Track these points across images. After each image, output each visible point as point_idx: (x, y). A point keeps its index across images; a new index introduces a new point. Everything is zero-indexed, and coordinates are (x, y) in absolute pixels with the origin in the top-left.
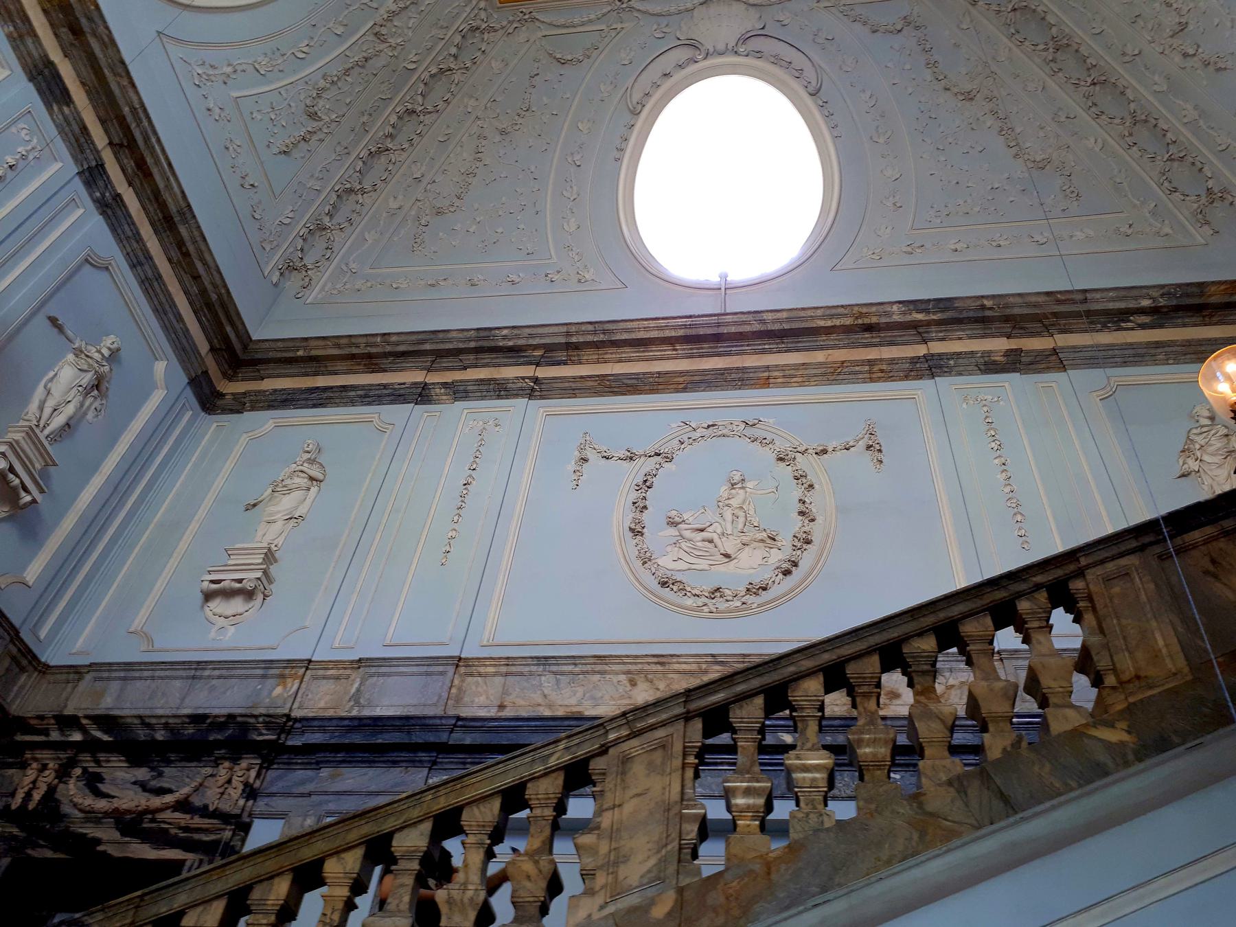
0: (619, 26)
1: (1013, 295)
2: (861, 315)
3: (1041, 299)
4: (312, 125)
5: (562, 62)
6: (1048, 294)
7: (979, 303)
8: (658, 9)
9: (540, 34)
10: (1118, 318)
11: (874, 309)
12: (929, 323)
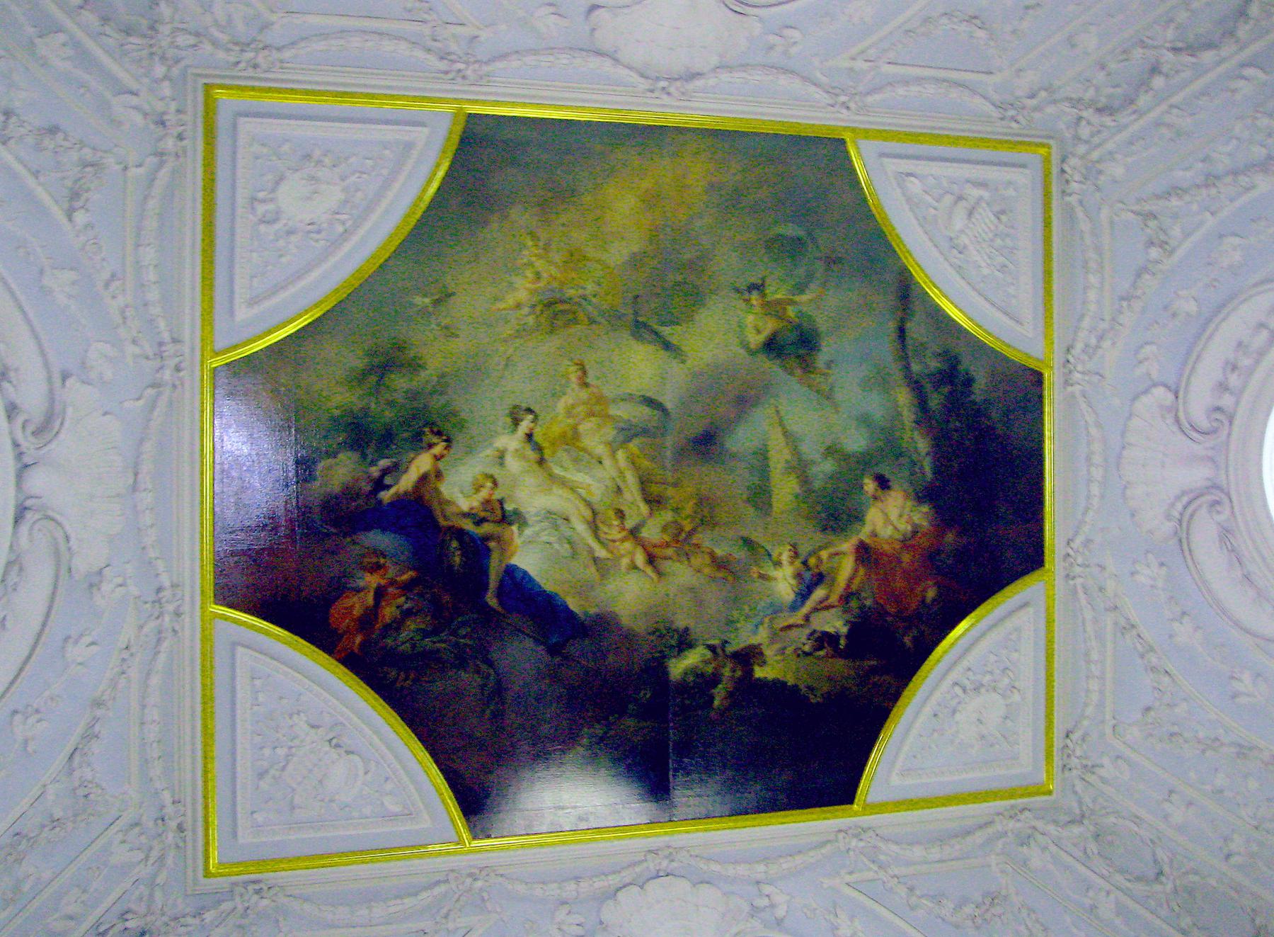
0: (860, 65)
8: (783, 81)
9: (997, 78)
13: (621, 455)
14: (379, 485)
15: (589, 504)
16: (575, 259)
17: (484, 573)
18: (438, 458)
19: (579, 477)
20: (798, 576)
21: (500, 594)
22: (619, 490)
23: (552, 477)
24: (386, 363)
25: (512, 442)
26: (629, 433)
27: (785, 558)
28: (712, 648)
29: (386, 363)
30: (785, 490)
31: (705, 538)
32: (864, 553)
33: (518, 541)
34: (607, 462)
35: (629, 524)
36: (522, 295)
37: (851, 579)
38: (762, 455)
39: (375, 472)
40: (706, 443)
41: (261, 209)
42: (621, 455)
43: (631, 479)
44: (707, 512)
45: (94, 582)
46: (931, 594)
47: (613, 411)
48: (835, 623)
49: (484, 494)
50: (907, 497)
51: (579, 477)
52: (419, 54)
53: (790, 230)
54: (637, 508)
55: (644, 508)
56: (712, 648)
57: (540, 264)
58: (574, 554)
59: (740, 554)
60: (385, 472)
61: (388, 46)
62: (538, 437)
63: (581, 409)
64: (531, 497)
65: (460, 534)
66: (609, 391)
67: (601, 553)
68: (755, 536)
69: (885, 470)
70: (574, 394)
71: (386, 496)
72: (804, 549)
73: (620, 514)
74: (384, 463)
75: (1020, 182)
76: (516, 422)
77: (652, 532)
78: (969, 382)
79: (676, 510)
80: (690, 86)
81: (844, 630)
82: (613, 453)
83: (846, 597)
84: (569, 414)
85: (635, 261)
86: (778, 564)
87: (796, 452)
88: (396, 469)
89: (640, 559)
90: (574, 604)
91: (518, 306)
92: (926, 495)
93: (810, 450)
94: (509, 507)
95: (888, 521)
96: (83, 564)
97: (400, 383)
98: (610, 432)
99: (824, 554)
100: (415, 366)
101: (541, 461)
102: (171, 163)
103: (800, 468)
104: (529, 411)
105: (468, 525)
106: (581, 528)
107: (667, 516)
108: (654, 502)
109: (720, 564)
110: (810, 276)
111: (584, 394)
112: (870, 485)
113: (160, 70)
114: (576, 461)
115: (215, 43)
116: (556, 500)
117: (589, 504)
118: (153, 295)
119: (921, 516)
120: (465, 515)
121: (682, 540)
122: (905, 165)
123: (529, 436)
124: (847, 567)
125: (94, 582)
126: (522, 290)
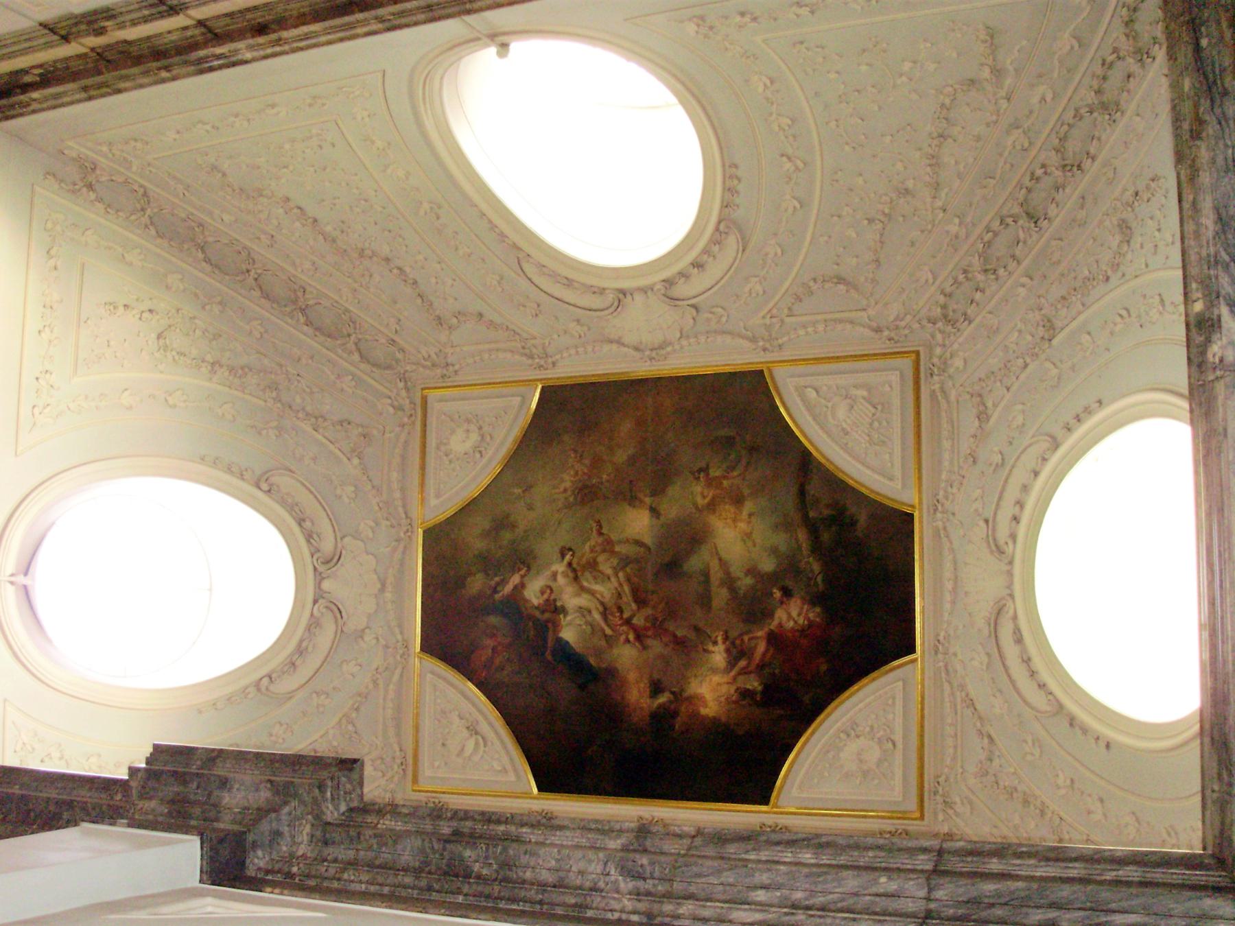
0: (768, 321)
1: (150, 85)
2: (278, 42)
3: (122, 85)
4: (1128, 215)
5: (840, 280)
6: (119, 91)
7: (175, 72)
9: (871, 312)
10: (50, 77)
11: (269, 51)
12: (205, 45)
13: (621, 574)
14: (495, 590)
15: (602, 604)
16: (597, 462)
17: (545, 640)
18: (522, 577)
19: (597, 587)
20: (728, 651)
21: (554, 653)
22: (619, 596)
23: (583, 589)
24: (502, 524)
25: (560, 567)
26: (625, 562)
27: (720, 638)
28: (673, 693)
29: (502, 524)
30: (721, 597)
31: (671, 626)
32: (775, 639)
33: (563, 623)
34: (613, 579)
35: (626, 616)
36: (568, 484)
37: (764, 655)
38: (706, 574)
39: (493, 583)
40: (672, 568)
41: (443, 448)
42: (621, 574)
43: (626, 589)
44: (672, 610)
45: (360, 635)
46: (824, 668)
47: (617, 549)
48: (754, 684)
49: (546, 596)
50: (804, 600)
51: (597, 587)
52: (517, 357)
53: (723, 432)
54: (630, 607)
55: (634, 606)
56: (673, 693)
57: (578, 466)
58: (593, 632)
59: (692, 635)
60: (498, 584)
61: (501, 355)
62: (575, 566)
63: (598, 548)
64: (571, 600)
65: (531, 617)
66: (614, 537)
67: (608, 631)
68: (701, 625)
69: (789, 583)
70: (595, 539)
71: (497, 597)
72: (733, 634)
73: (620, 610)
74: (497, 579)
75: (891, 380)
76: (563, 556)
77: (638, 621)
78: (853, 523)
79: (654, 607)
80: (662, 352)
81: (760, 688)
82: (616, 575)
83: (761, 667)
84: (592, 551)
85: (632, 460)
86: (715, 643)
87: (728, 573)
88: (503, 582)
89: (631, 637)
90: (592, 661)
91: (565, 490)
92: (816, 599)
93: (737, 570)
94: (559, 604)
95: (790, 617)
96: (353, 624)
97: (507, 536)
98: (615, 561)
99: (746, 638)
100: (513, 526)
101: (576, 579)
102: (407, 428)
103: (730, 582)
104: (570, 549)
105: (537, 614)
106: (597, 616)
107: (648, 611)
108: (641, 601)
109: (680, 643)
110: (739, 461)
111: (600, 540)
112: (777, 594)
113: (401, 385)
114: (595, 578)
115: (424, 367)
116: (584, 601)
117: (602, 604)
118: (398, 495)
119: (815, 614)
120: (537, 608)
121: (657, 627)
122: (802, 381)
123: (570, 564)
124: (761, 647)
125: (360, 635)
126: (568, 480)
